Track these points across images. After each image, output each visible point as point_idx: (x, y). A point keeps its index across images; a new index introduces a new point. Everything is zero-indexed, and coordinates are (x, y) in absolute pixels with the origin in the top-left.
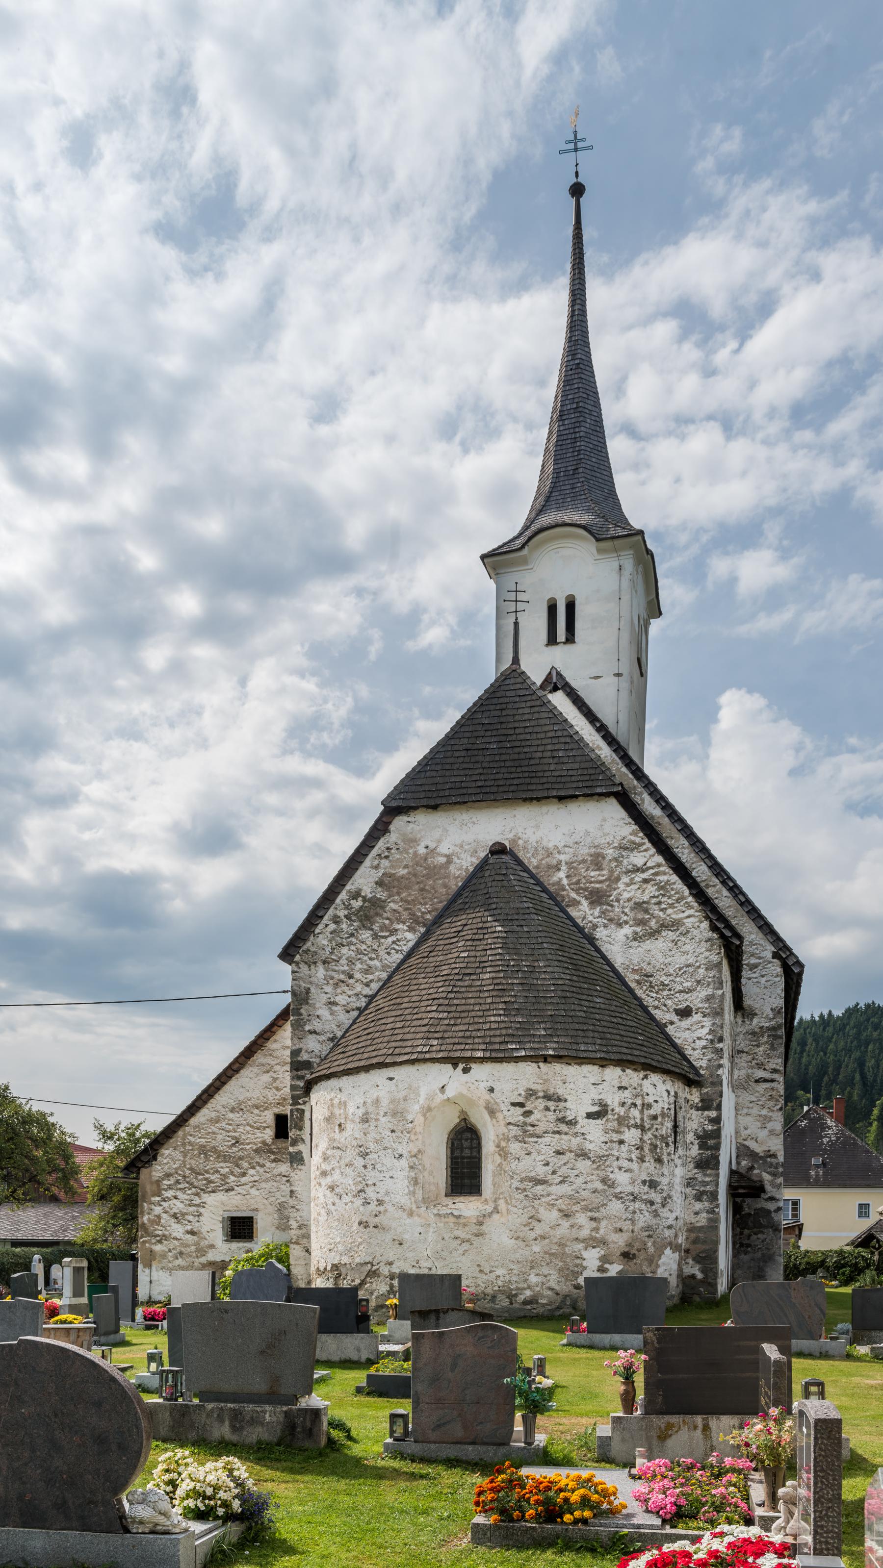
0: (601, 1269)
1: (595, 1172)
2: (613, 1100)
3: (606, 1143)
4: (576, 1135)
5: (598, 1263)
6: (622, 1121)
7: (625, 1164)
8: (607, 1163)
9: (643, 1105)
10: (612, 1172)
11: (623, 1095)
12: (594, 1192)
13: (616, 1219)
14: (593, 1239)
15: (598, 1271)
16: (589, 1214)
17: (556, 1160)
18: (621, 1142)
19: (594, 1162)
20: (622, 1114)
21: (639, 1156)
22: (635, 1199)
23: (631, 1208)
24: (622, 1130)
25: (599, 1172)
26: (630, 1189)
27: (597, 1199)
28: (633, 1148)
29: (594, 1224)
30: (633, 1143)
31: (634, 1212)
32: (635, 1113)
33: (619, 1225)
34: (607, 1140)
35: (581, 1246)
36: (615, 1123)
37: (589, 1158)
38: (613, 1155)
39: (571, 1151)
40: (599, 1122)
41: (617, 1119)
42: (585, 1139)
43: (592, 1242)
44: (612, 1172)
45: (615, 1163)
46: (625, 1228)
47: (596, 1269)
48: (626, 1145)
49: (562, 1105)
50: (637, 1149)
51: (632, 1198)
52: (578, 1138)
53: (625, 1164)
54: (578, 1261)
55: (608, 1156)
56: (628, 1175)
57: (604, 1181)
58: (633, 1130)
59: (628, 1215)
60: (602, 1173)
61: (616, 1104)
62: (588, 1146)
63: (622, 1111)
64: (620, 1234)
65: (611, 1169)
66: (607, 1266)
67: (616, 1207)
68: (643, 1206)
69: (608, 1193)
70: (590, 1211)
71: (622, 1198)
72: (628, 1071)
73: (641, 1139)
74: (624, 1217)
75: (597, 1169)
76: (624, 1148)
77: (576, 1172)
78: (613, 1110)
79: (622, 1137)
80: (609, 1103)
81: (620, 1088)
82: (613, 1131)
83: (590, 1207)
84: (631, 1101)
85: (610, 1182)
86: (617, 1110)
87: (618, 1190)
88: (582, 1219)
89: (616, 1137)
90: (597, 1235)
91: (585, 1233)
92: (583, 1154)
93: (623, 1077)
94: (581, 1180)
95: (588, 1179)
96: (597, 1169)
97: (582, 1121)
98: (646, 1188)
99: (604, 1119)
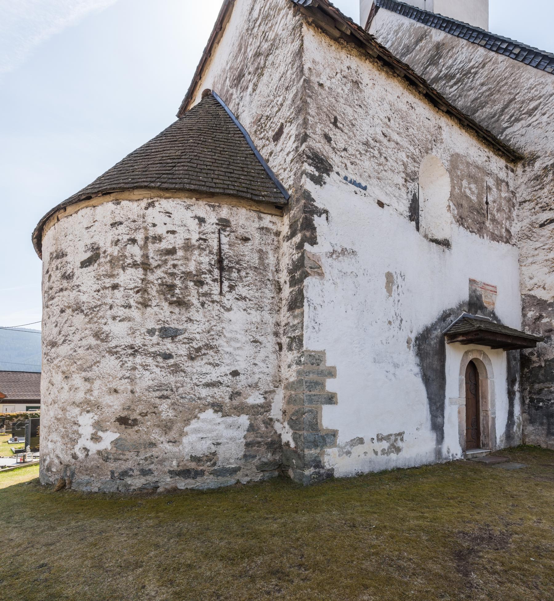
0: (95, 438)
1: (89, 326)
2: (105, 240)
3: (99, 291)
4: (72, 288)
5: (91, 430)
6: (113, 262)
7: (121, 312)
8: (99, 315)
9: (147, 238)
10: (105, 324)
11: (117, 232)
12: (88, 349)
13: (111, 378)
14: (88, 402)
15: (92, 439)
16: (83, 374)
17: (60, 319)
18: (115, 287)
19: (86, 315)
20: (116, 254)
21: (141, 300)
22: (135, 351)
23: (130, 364)
24: (115, 273)
25: (91, 325)
26: (129, 341)
27: (92, 356)
28: (131, 292)
29: (88, 385)
30: (132, 286)
31: (134, 369)
32: (136, 251)
33: (113, 385)
34: (98, 287)
35: (77, 410)
36: (108, 267)
37: (82, 311)
38: (106, 304)
39: (69, 307)
40: (90, 268)
41: (110, 262)
42: (79, 291)
43: (89, 406)
44: (105, 324)
45: (109, 313)
46: (121, 388)
47: (89, 437)
48: (122, 289)
49: (65, 259)
50: (138, 292)
51: (130, 351)
52: (74, 292)
53: (121, 312)
54: (75, 428)
55: (100, 305)
56: (126, 324)
57: (97, 335)
58: (130, 271)
59: (124, 372)
60: (94, 327)
61: (108, 244)
62: (83, 298)
63: (115, 251)
64: (115, 395)
65: (104, 321)
66: (100, 434)
67: (110, 363)
68: (150, 360)
69: (101, 349)
70: (85, 371)
71: (116, 353)
72: (124, 203)
73: (143, 280)
74: (120, 375)
75: (89, 322)
76: (118, 294)
77: (73, 329)
78: (105, 252)
79: (116, 281)
80: (101, 245)
81: (113, 225)
82: (106, 276)
83: (85, 367)
84: (128, 237)
85: (103, 336)
86: (109, 250)
87: (113, 344)
88: (77, 380)
89: (108, 282)
90: (92, 398)
91: (80, 396)
92: (78, 309)
93: (117, 212)
94: (78, 336)
95: (83, 335)
96: (89, 322)
97: (78, 272)
98: (155, 339)
99: (96, 265)
